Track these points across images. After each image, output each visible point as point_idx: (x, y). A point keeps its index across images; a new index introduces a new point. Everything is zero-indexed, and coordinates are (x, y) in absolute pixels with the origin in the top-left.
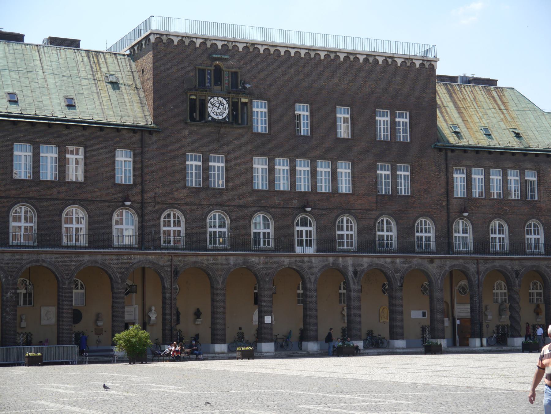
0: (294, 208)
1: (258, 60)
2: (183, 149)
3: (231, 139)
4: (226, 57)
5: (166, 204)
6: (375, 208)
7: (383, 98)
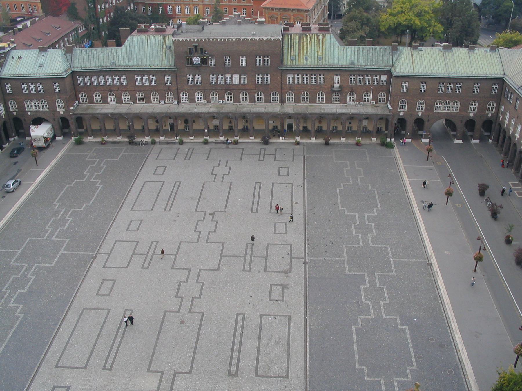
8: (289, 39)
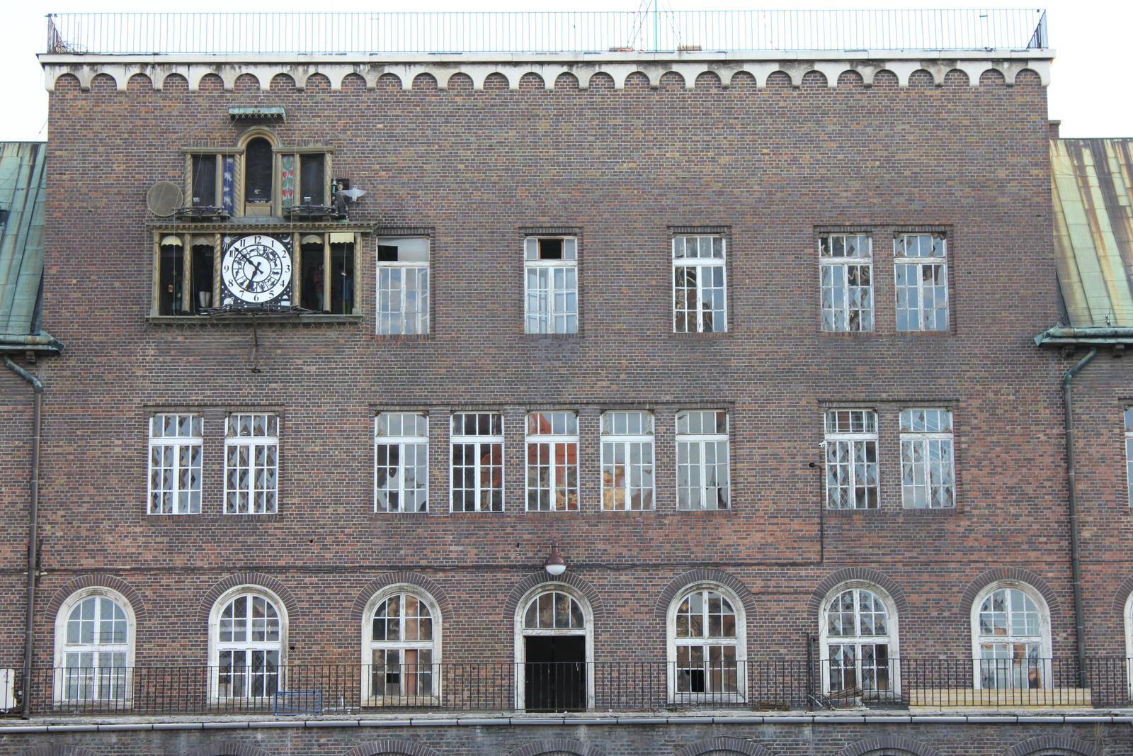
0: (514, 567)
1: (398, 112)
2: (137, 400)
3: (299, 362)
4: (274, 111)
5: (75, 572)
6: (815, 557)
7: (845, 194)
8: (1091, 172)
